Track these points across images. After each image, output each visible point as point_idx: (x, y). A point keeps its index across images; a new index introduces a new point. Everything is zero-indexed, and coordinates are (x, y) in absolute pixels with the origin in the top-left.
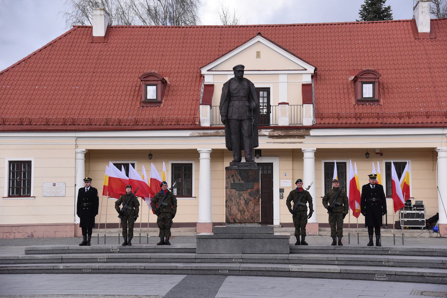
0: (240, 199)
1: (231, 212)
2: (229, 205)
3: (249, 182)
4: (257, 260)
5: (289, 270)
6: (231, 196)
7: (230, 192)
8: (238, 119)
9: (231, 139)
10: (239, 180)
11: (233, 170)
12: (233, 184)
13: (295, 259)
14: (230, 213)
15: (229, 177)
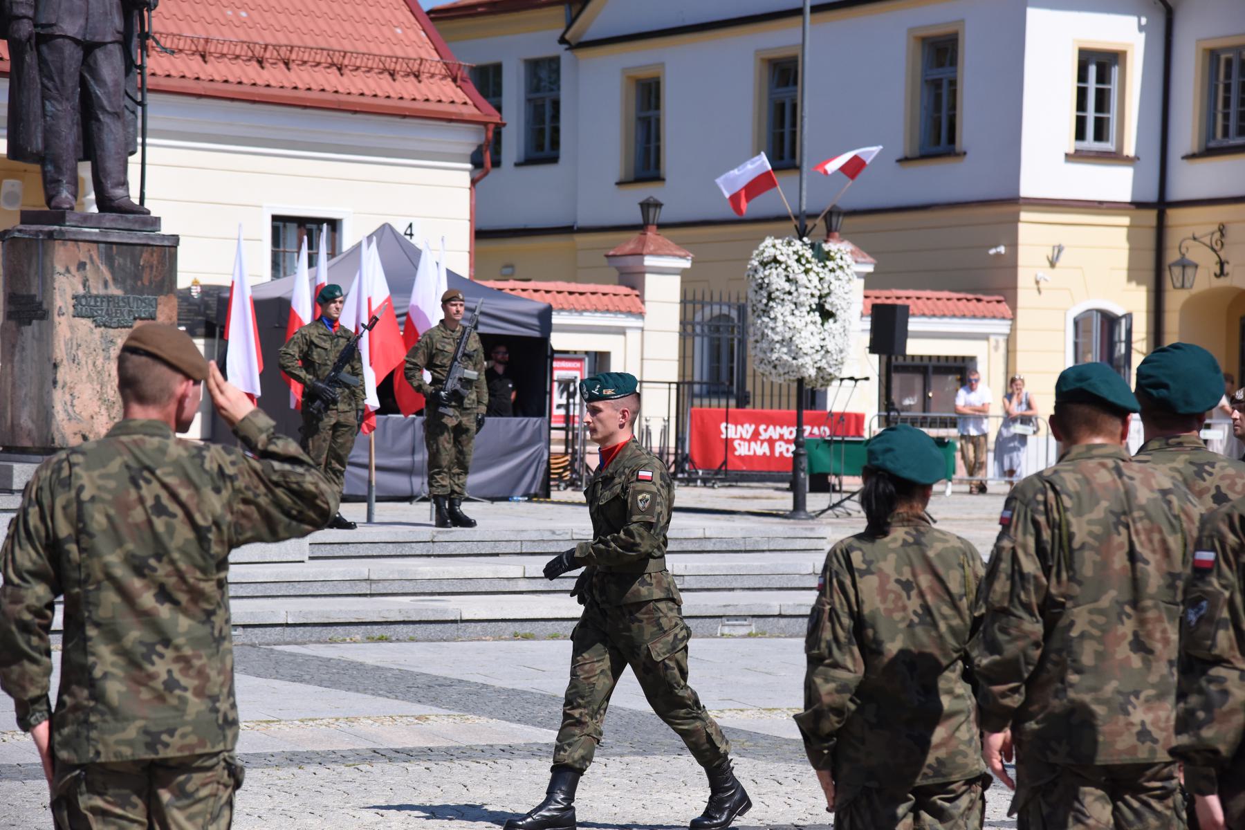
0: (109, 358)
1: (72, 406)
2: (68, 379)
3: (142, 293)
4: (259, 586)
5: (458, 618)
6: (75, 343)
7: (71, 327)
8: (84, 35)
9: (44, 115)
10: (106, 284)
11: (80, 244)
12: (84, 296)
13: (391, 577)
14: (70, 409)
15: (68, 271)
